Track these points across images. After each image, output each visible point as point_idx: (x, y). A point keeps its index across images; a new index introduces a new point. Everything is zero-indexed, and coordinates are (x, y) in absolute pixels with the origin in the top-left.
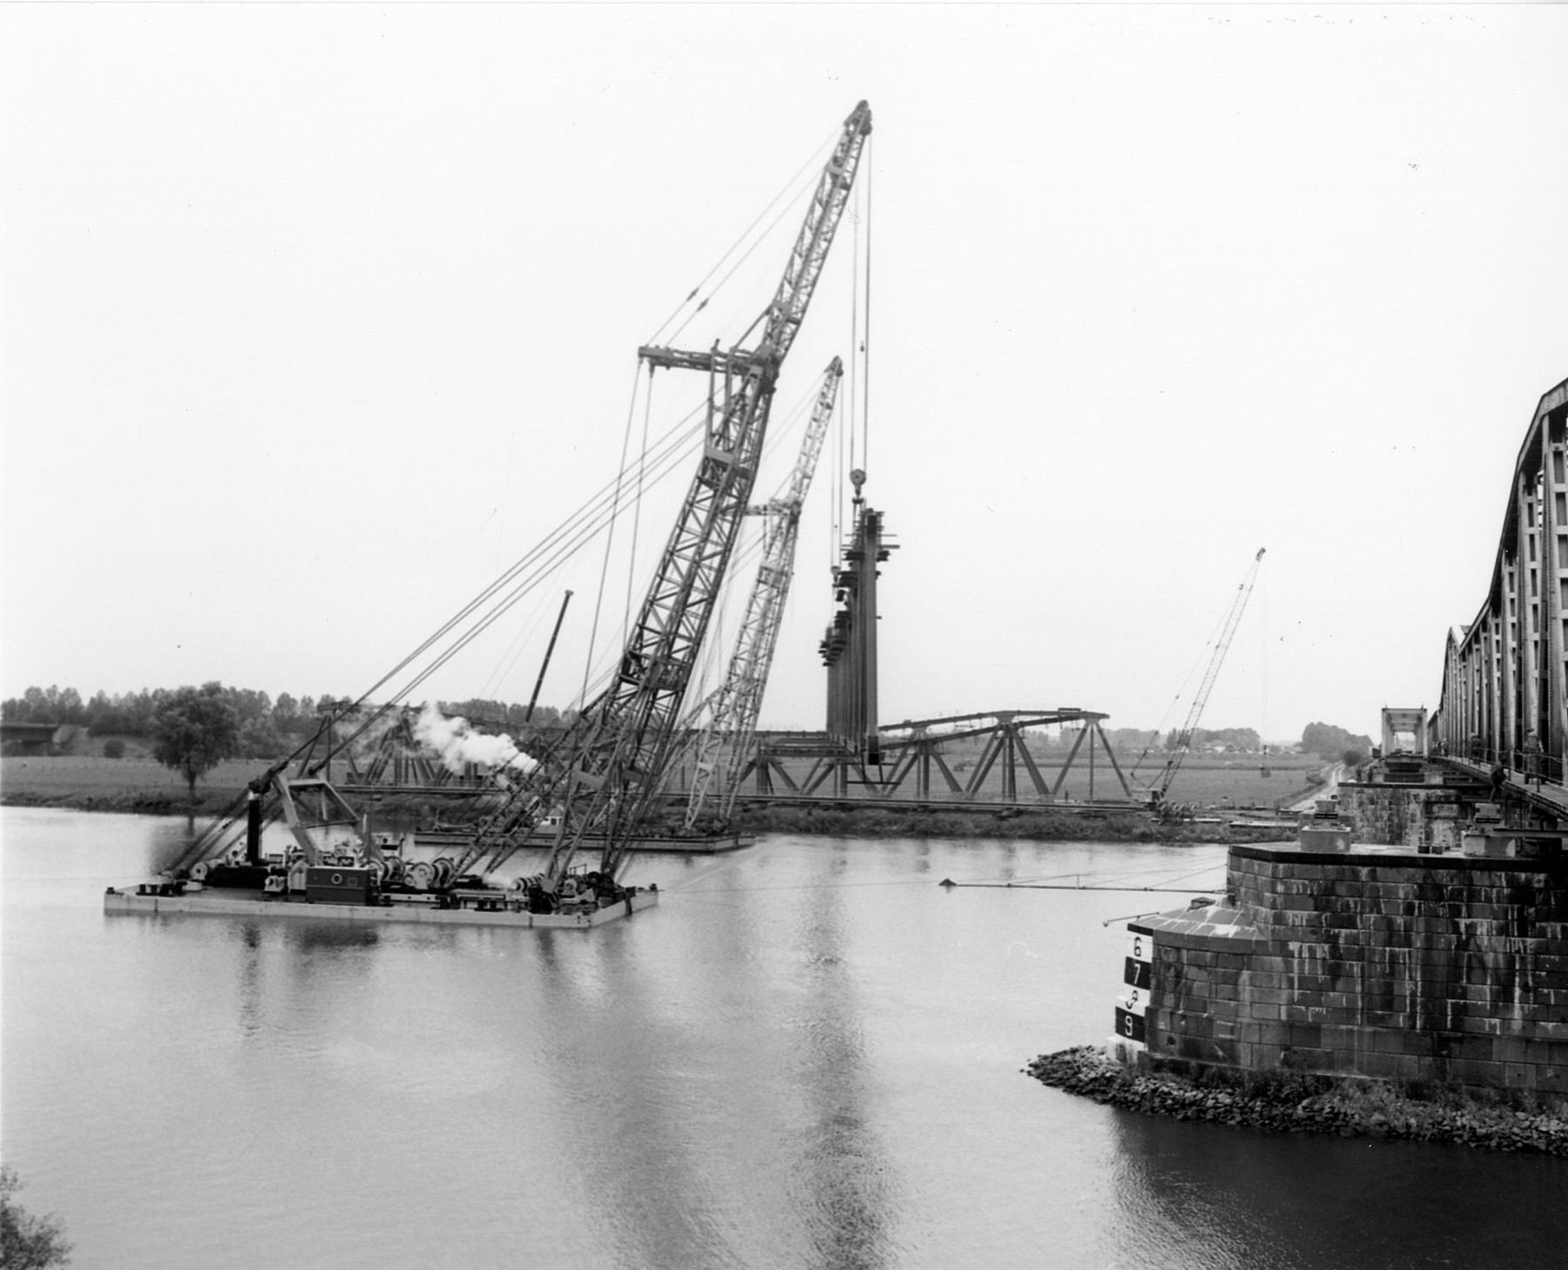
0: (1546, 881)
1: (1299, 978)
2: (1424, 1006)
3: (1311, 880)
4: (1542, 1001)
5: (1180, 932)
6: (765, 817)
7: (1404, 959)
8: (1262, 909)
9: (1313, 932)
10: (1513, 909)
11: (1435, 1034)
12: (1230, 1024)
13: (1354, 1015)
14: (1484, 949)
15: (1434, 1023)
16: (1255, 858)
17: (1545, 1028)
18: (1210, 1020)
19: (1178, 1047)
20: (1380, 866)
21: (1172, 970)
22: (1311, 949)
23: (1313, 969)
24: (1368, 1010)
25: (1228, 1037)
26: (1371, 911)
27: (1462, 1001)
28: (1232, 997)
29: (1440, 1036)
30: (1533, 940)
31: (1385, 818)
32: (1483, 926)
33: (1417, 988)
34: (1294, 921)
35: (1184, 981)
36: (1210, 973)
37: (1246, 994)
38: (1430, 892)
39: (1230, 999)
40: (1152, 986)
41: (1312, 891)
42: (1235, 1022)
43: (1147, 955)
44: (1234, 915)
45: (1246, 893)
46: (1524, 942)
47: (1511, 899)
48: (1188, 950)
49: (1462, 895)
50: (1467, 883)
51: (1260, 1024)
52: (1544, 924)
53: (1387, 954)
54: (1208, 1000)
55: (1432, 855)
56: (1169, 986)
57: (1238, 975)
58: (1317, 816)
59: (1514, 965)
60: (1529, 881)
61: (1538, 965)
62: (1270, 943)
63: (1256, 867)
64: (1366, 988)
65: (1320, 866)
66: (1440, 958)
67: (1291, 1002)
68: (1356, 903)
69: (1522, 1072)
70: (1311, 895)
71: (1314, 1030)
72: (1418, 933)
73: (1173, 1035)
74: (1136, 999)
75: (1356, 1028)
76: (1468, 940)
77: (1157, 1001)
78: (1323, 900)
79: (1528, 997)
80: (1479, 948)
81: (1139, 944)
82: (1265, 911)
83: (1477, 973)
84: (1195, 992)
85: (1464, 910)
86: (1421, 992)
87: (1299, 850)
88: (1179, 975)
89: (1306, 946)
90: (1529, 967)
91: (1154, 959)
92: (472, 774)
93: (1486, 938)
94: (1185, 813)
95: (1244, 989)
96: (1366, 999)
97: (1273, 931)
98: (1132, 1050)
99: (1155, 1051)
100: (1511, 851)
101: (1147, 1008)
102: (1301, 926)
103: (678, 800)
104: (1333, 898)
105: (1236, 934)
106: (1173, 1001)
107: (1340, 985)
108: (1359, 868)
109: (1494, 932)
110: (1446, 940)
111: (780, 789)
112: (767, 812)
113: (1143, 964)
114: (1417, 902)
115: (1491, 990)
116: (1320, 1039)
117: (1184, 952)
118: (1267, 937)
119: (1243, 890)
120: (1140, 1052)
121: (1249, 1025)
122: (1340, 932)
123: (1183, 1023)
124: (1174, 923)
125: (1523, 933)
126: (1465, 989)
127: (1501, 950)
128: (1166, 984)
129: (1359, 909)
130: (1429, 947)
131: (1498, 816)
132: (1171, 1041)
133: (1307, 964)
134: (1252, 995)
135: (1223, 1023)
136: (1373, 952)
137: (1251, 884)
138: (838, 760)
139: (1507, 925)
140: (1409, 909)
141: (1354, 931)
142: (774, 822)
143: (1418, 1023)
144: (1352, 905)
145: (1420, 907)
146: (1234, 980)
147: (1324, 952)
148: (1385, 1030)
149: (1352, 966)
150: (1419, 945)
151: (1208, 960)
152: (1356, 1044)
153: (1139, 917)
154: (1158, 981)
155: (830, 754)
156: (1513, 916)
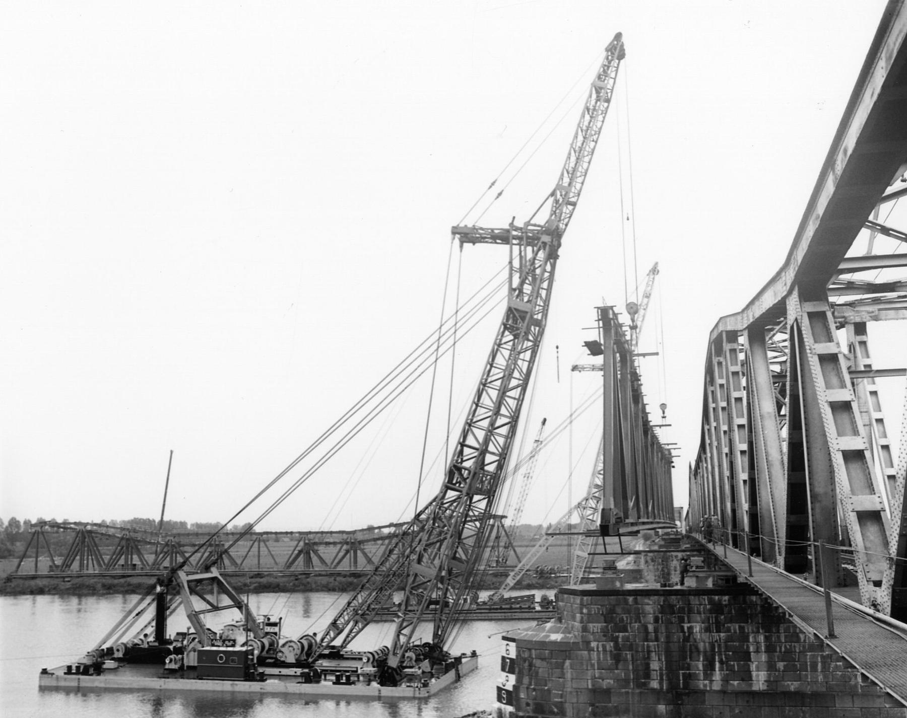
0: (729, 600)
1: (598, 663)
2: (668, 676)
3: (601, 606)
4: (731, 669)
5: (531, 639)
6: (308, 583)
7: (655, 648)
8: (576, 623)
9: (604, 636)
10: (712, 618)
11: (674, 692)
12: (560, 692)
13: (629, 683)
14: (698, 641)
15: (673, 686)
16: (571, 594)
17: (733, 685)
18: (549, 691)
19: (531, 708)
20: (639, 595)
21: (527, 662)
22: (604, 647)
24: (636, 679)
25: (560, 700)
26: (636, 622)
27: (688, 672)
28: (560, 676)
29: (676, 692)
30: (724, 634)
31: (660, 569)
32: (697, 628)
33: (663, 665)
34: (593, 630)
35: (533, 668)
36: (548, 663)
37: (569, 676)
38: (668, 609)
39: (560, 678)
40: (516, 672)
41: (602, 612)
42: (563, 691)
43: (513, 655)
44: (560, 628)
45: (567, 614)
46: (719, 636)
47: (711, 611)
48: (536, 649)
49: (684, 610)
50: (687, 603)
51: (577, 692)
52: (729, 625)
53: (646, 646)
54: (547, 679)
55: (667, 588)
56: (526, 672)
57: (564, 663)
58: (605, 569)
59: (715, 649)
60: (720, 600)
61: (727, 649)
62: (581, 643)
63: (572, 600)
64: (635, 666)
65: (606, 597)
66: (674, 647)
67: (594, 678)
68: (627, 617)
69: (722, 711)
70: (602, 614)
71: (607, 692)
72: (662, 633)
73: (528, 701)
74: (507, 681)
75: (630, 691)
76: (689, 635)
77: (519, 681)
78: (608, 617)
79: (723, 667)
80: (695, 640)
81: (508, 648)
82: (577, 625)
83: (695, 654)
84: (540, 674)
85: (686, 619)
86: (666, 668)
87: (595, 589)
88: (531, 665)
89: (600, 644)
90: (723, 650)
91: (517, 656)
92: (129, 563)
93: (699, 634)
94: (552, 571)
95: (567, 672)
96: (635, 673)
97: (582, 637)
98: (506, 711)
99: (519, 711)
100: (710, 584)
101: (514, 686)
102: (598, 632)
103: (256, 575)
104: (614, 615)
105: (562, 638)
106: (528, 680)
107: (620, 666)
108: (628, 597)
109: (703, 631)
110: (677, 636)
111: (317, 566)
112: (308, 580)
113: (510, 659)
114: (660, 615)
115: (703, 665)
116: (610, 698)
117: (533, 651)
118: (579, 640)
119: (565, 613)
120: (510, 713)
121: (571, 692)
122: (619, 635)
123: (534, 693)
124: (527, 634)
125: (718, 631)
126: (689, 665)
127: (707, 640)
128: (524, 671)
129: (629, 620)
130: (668, 641)
131: (703, 565)
132: (528, 704)
133: (601, 654)
134: (572, 675)
135: (556, 692)
136: (637, 645)
137: (570, 609)
138: (351, 548)
139: (709, 626)
140: (656, 620)
141: (627, 634)
142: (314, 586)
143: (665, 685)
144: (625, 619)
145: (662, 618)
146: (561, 666)
147: (611, 647)
148: (646, 691)
149: (626, 654)
150: (662, 640)
151: (547, 655)
152: (631, 700)
153: (508, 632)
154: (519, 668)
155: (347, 543)
156: (712, 621)
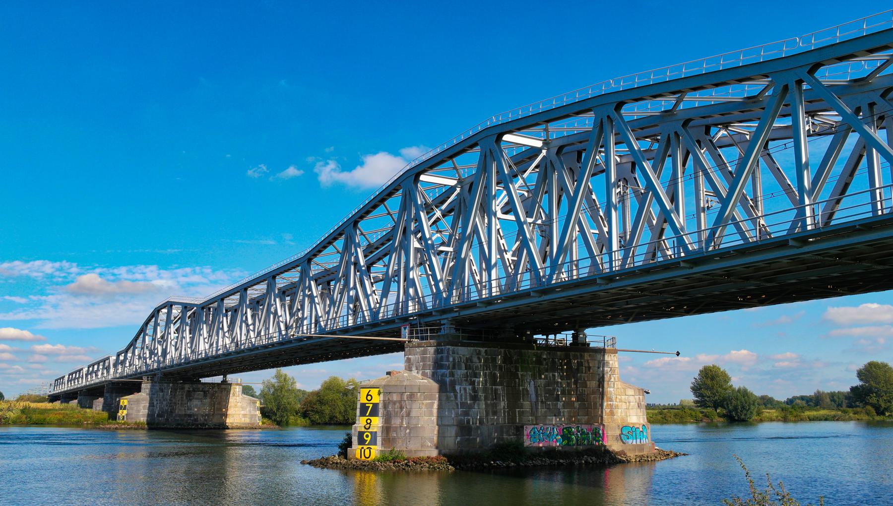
23: (466, 399)
26: (487, 370)
114: (503, 365)
